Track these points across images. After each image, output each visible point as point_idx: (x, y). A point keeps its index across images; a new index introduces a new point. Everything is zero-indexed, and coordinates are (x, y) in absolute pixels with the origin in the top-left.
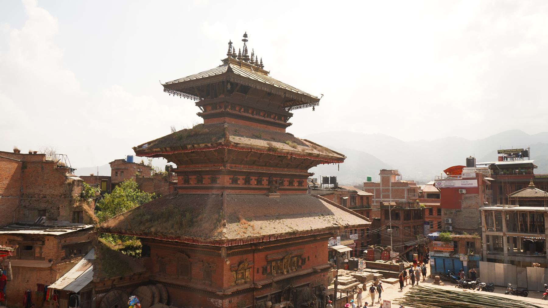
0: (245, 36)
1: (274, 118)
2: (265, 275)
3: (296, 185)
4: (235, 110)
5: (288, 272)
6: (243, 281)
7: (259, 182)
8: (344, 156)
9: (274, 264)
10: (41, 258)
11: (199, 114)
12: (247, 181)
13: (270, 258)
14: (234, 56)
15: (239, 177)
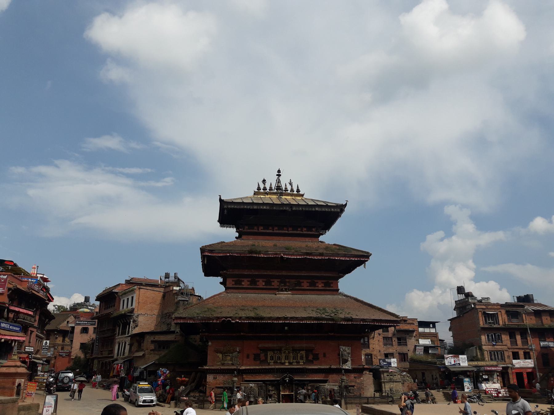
0: (279, 171)
1: (302, 231)
2: (258, 362)
3: (320, 286)
4: (254, 229)
5: (290, 363)
6: (230, 362)
7: (268, 283)
8: (368, 253)
9: (270, 354)
10: (142, 350)
11: (236, 238)
12: (253, 282)
13: (260, 346)
14: (265, 189)
15: (243, 279)
